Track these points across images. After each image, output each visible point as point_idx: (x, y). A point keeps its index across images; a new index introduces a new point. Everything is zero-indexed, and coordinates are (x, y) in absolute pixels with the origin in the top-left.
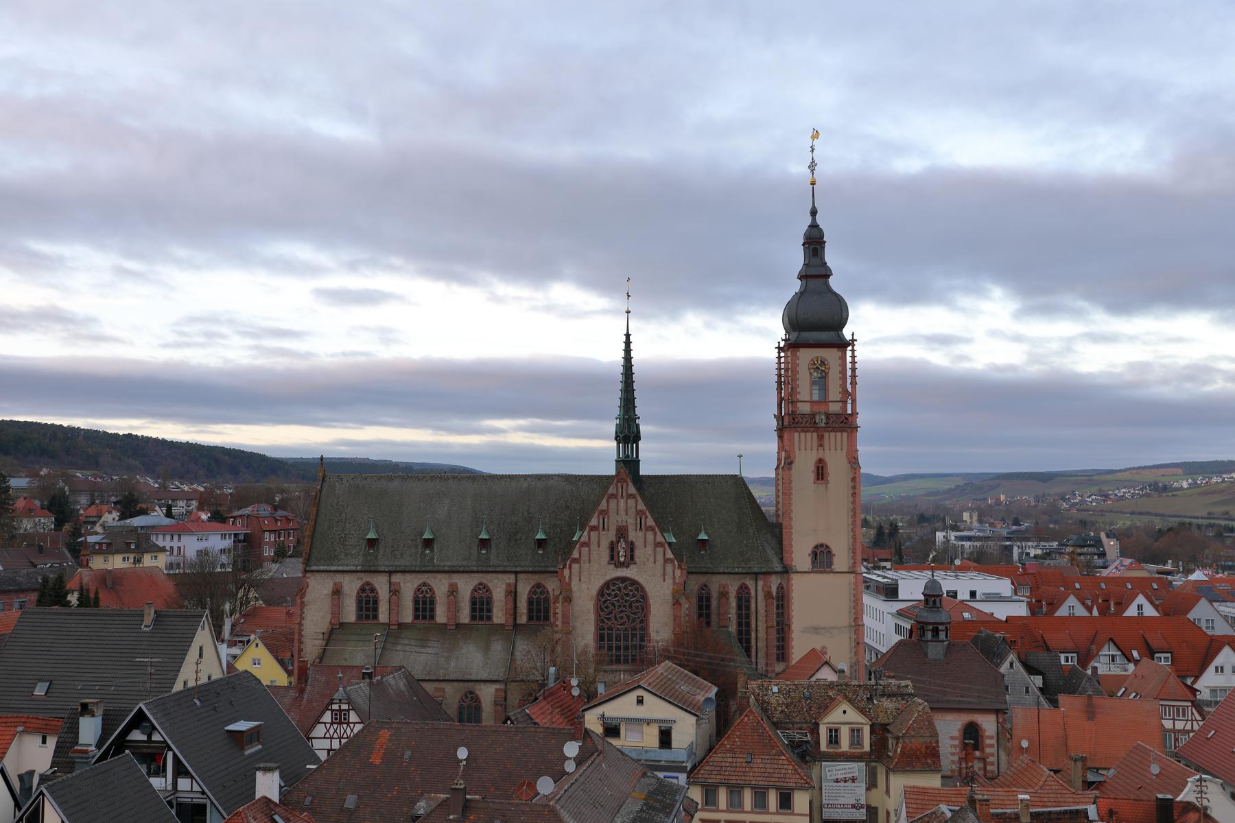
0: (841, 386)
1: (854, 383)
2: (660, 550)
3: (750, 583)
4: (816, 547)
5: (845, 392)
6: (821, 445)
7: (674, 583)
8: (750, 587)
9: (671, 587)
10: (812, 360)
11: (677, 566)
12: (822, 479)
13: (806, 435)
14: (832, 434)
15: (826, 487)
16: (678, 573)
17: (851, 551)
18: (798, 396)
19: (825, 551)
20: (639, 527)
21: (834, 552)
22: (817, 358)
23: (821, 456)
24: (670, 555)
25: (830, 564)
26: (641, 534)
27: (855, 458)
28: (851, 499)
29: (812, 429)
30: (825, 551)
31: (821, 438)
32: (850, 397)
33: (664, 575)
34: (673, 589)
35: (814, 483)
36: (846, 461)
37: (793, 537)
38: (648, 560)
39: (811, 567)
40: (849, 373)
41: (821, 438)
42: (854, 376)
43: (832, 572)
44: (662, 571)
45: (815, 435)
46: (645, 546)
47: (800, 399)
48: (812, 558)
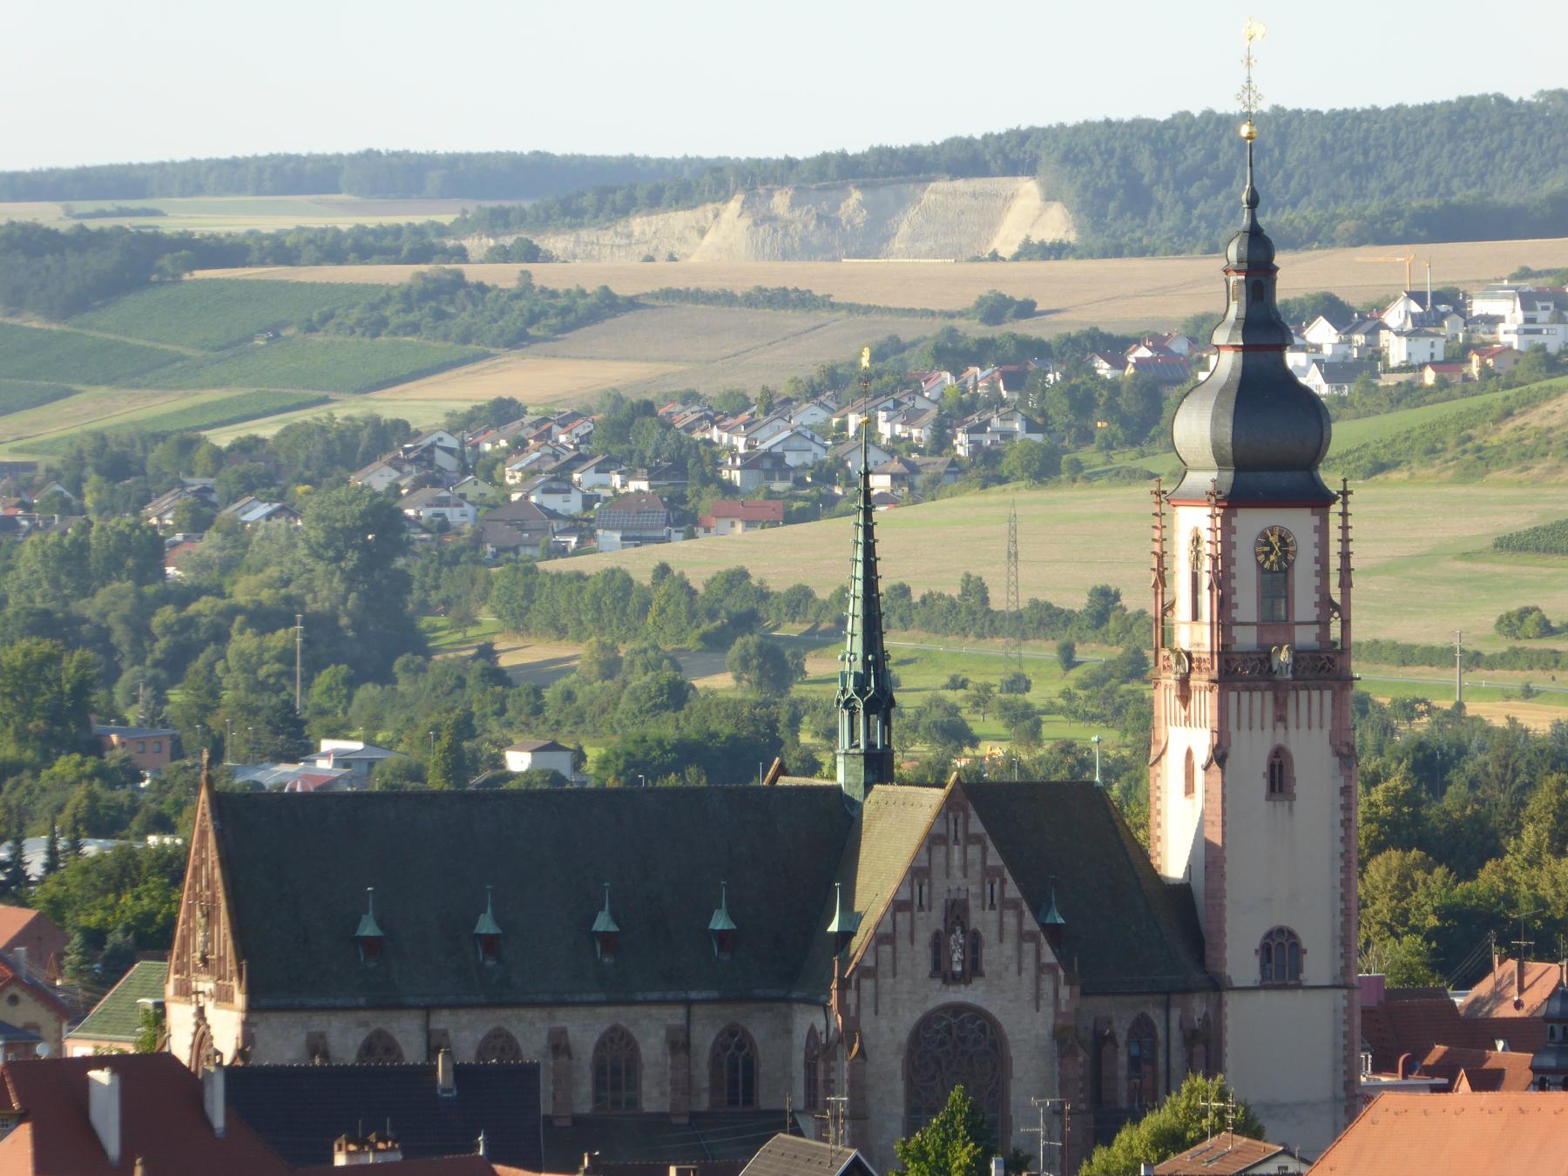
0: (1318, 589)
1: (1345, 584)
2: (1029, 947)
3: (1156, 1015)
4: (1270, 935)
5: (1326, 604)
6: (1281, 718)
7: (1057, 1014)
8: (1155, 1021)
9: (1051, 1021)
10: (1263, 535)
11: (1062, 978)
12: (1281, 790)
13: (1251, 696)
14: (1303, 694)
15: (1291, 808)
16: (1065, 992)
17: (1338, 942)
18: (1234, 613)
19: (1287, 945)
20: (988, 901)
21: (1304, 945)
22: (1272, 530)
23: (1280, 740)
24: (1049, 957)
25: (1298, 969)
26: (992, 916)
27: (1348, 744)
28: (1341, 832)
29: (1263, 684)
30: (1287, 945)
31: (1280, 705)
32: (1336, 614)
33: (1037, 998)
34: (1054, 1025)
35: (1268, 798)
36: (1328, 750)
37: (1228, 914)
38: (1007, 969)
39: (1259, 978)
40: (1335, 563)
41: (1280, 705)
42: (1346, 570)
43: (1299, 986)
44: (1033, 991)
45: (1269, 695)
46: (1001, 941)
47: (1238, 620)
48: (1261, 960)
